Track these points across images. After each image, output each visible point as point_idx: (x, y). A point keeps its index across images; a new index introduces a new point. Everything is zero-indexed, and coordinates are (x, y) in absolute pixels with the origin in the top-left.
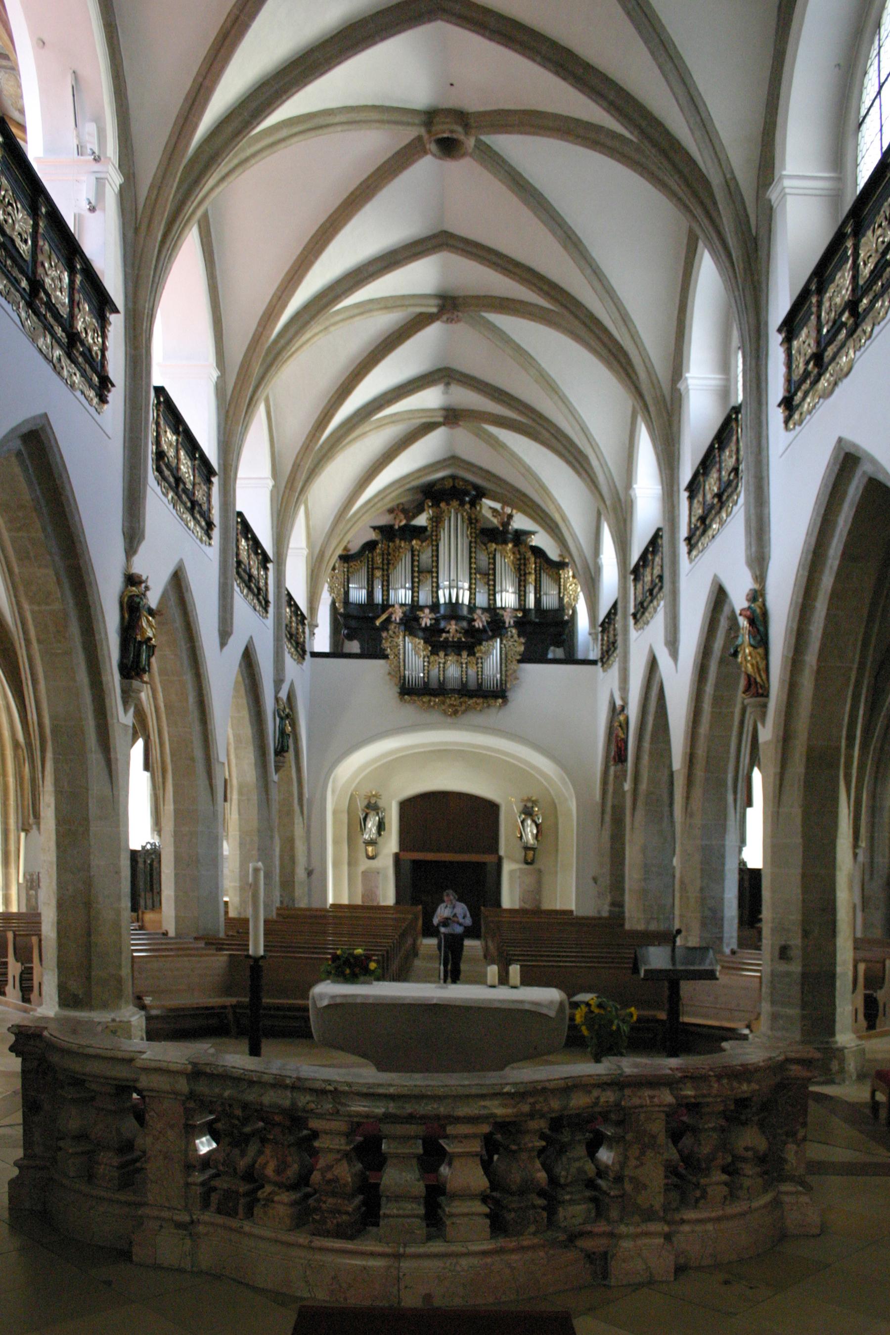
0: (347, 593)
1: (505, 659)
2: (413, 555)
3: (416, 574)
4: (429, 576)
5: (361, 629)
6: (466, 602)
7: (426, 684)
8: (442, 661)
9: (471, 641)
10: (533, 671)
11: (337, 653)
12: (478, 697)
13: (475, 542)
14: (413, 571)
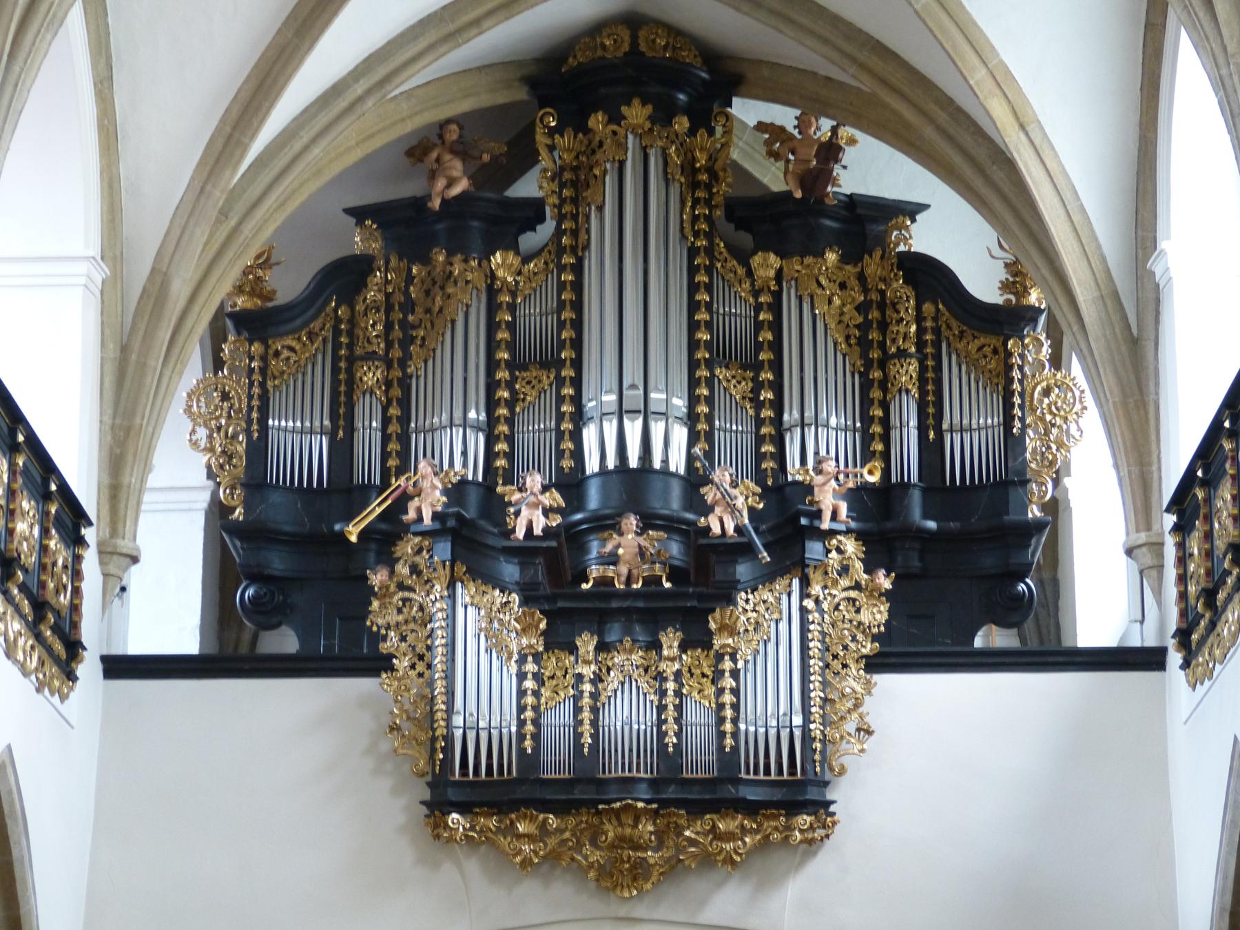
1: (819, 663)
3: (503, 375)
4: (547, 378)
6: (678, 463)
7: (529, 762)
8: (588, 671)
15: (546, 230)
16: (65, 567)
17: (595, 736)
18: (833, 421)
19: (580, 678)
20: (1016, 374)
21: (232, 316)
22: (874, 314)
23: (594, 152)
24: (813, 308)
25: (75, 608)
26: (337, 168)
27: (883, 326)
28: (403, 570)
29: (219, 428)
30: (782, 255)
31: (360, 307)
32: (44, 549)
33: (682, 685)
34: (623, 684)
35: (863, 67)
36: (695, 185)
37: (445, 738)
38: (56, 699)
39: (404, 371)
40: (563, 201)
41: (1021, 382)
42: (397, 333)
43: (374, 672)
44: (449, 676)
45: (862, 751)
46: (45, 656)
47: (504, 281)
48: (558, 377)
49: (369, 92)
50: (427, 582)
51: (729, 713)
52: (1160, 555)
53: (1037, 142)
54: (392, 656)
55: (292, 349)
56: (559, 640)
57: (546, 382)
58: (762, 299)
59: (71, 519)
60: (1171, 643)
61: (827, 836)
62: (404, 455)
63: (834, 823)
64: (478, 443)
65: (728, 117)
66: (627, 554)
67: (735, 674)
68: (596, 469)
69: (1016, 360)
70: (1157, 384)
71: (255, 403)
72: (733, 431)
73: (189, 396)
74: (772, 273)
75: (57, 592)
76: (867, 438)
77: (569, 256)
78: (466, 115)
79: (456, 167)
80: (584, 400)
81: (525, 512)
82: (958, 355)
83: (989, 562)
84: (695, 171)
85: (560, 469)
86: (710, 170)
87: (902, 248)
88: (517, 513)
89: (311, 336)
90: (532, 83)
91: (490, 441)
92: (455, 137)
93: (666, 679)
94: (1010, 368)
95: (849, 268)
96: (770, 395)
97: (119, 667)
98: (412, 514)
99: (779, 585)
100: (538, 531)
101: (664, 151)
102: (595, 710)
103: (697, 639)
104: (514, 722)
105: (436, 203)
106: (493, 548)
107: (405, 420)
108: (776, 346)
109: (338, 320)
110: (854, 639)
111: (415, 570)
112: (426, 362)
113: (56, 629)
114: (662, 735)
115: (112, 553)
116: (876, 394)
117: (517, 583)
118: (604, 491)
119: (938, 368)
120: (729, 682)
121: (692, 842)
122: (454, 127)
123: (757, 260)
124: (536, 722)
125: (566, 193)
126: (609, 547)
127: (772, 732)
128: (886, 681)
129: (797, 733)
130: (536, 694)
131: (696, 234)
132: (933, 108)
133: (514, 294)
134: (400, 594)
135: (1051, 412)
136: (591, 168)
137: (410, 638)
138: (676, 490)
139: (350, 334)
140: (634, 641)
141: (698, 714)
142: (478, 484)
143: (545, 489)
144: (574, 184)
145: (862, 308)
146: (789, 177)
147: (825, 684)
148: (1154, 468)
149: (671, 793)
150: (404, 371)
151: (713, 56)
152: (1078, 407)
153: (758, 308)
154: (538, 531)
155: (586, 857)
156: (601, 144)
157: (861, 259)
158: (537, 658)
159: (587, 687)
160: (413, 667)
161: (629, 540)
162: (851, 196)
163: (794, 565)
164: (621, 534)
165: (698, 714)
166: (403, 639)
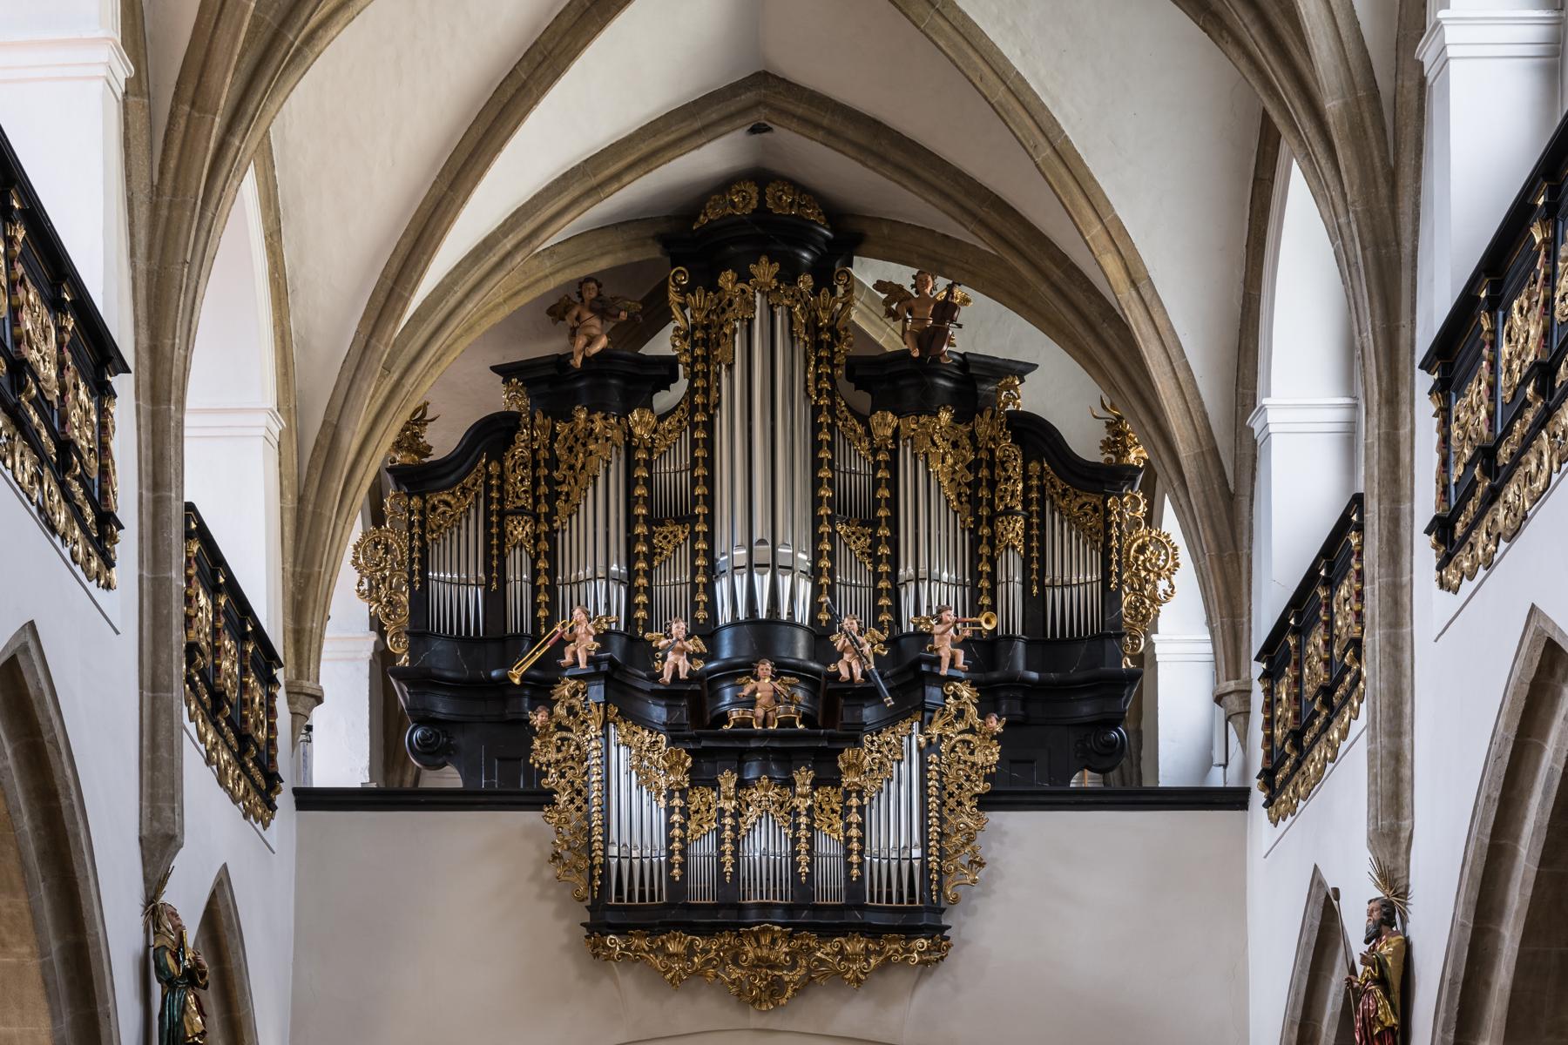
0: (420, 600)
1: (937, 803)
2: (630, 465)
3: (640, 530)
5: (464, 721)
7: (678, 888)
8: (729, 806)
9: (822, 737)
10: (1025, 840)
11: (387, 795)
12: (844, 930)
13: (832, 409)
14: (631, 521)
15: (680, 388)
16: (261, 704)
17: (736, 866)
18: (945, 575)
19: (721, 811)
20: (1114, 532)
21: (389, 470)
22: (984, 473)
23: (724, 311)
24: (927, 465)
25: (271, 743)
26: (486, 325)
27: (992, 484)
28: (560, 710)
29: (384, 579)
30: (899, 414)
31: (509, 463)
32: (244, 687)
33: (813, 820)
34: (760, 818)
35: (983, 223)
36: (818, 344)
37: (602, 866)
38: (259, 826)
39: (551, 527)
40: (695, 359)
41: (1119, 539)
42: (543, 489)
43: (537, 806)
44: (605, 811)
45: (974, 881)
46: (249, 786)
47: (641, 438)
48: (692, 532)
49: (517, 247)
50: (584, 722)
51: (855, 845)
52: (1247, 702)
53: (1147, 298)
54: (553, 791)
55: (447, 504)
56: (702, 778)
57: (681, 537)
58: (880, 457)
59: (264, 660)
60: (1255, 783)
61: (942, 958)
62: (552, 606)
63: (948, 947)
64: (619, 594)
65: (849, 275)
66: (764, 696)
67: (861, 810)
68: (728, 620)
69: (1115, 518)
70: (1251, 539)
71: (416, 555)
72: (854, 581)
73: (356, 548)
74: (889, 432)
75: (256, 727)
76: (976, 593)
77: (700, 414)
78: (602, 272)
79: (595, 324)
80: (717, 555)
81: (671, 657)
82: (1061, 513)
83: (1086, 709)
84: (819, 330)
85: (695, 620)
86: (832, 329)
87: (1010, 407)
88: (664, 659)
89: (464, 490)
90: (666, 241)
91: (631, 593)
92: (594, 295)
93: (799, 814)
94: (1108, 525)
95: (960, 427)
96: (887, 551)
97: (309, 799)
98: (568, 659)
99: (901, 728)
100: (683, 675)
101: (790, 314)
102: (735, 842)
103: (827, 777)
104: (663, 853)
105: (578, 361)
106: (642, 691)
107: (552, 572)
109: (489, 476)
110: (968, 778)
111: (571, 710)
112: (570, 516)
113: (257, 761)
114: (795, 865)
115: (299, 693)
116: (984, 550)
117: (665, 724)
118: (736, 641)
119: (1042, 526)
120: (854, 818)
121: (821, 961)
122: (592, 285)
123: (875, 419)
124: (683, 853)
125: (698, 352)
126: (747, 690)
127: (894, 863)
128: (995, 817)
129: (916, 864)
130: (683, 827)
131: (819, 393)
132: (1047, 264)
133: (650, 451)
134: (559, 734)
135: (1145, 569)
136: (721, 327)
137: (569, 774)
138: (801, 640)
139: (501, 489)
140: (771, 779)
141: (828, 846)
142: (621, 634)
143: (688, 637)
144: (705, 343)
145: (973, 467)
146: (907, 336)
147: (942, 820)
148: (1245, 619)
149: (804, 917)
150: (551, 527)
151: (836, 213)
152: (1170, 563)
153: (876, 466)
154: (683, 675)
155: (729, 975)
156: (730, 303)
157: (973, 419)
158: (684, 793)
159: (728, 821)
160: (572, 801)
161: (764, 685)
162: (963, 356)
163: (915, 709)
164: (757, 679)
165: (828, 846)
166: (562, 775)
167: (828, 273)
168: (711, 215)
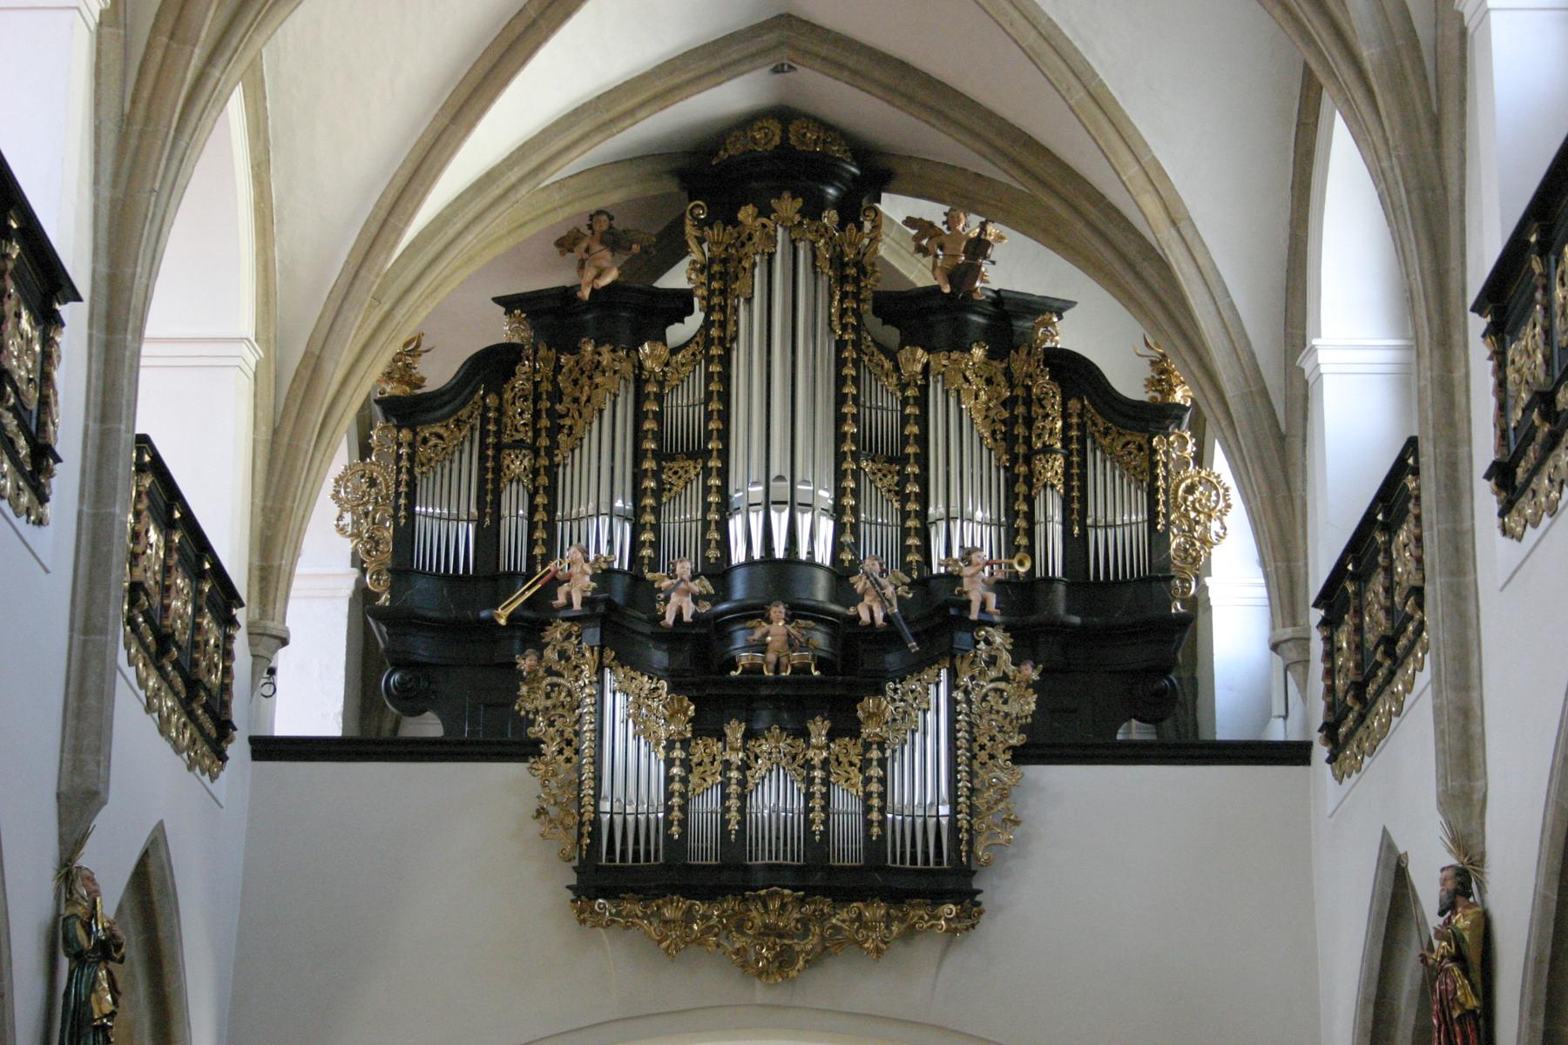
2: (640, 398)
13: (857, 345)
77: (716, 346)
79: (605, 256)
108: (923, 440)
151: (862, 151)
167: (855, 208)
168: (734, 149)
